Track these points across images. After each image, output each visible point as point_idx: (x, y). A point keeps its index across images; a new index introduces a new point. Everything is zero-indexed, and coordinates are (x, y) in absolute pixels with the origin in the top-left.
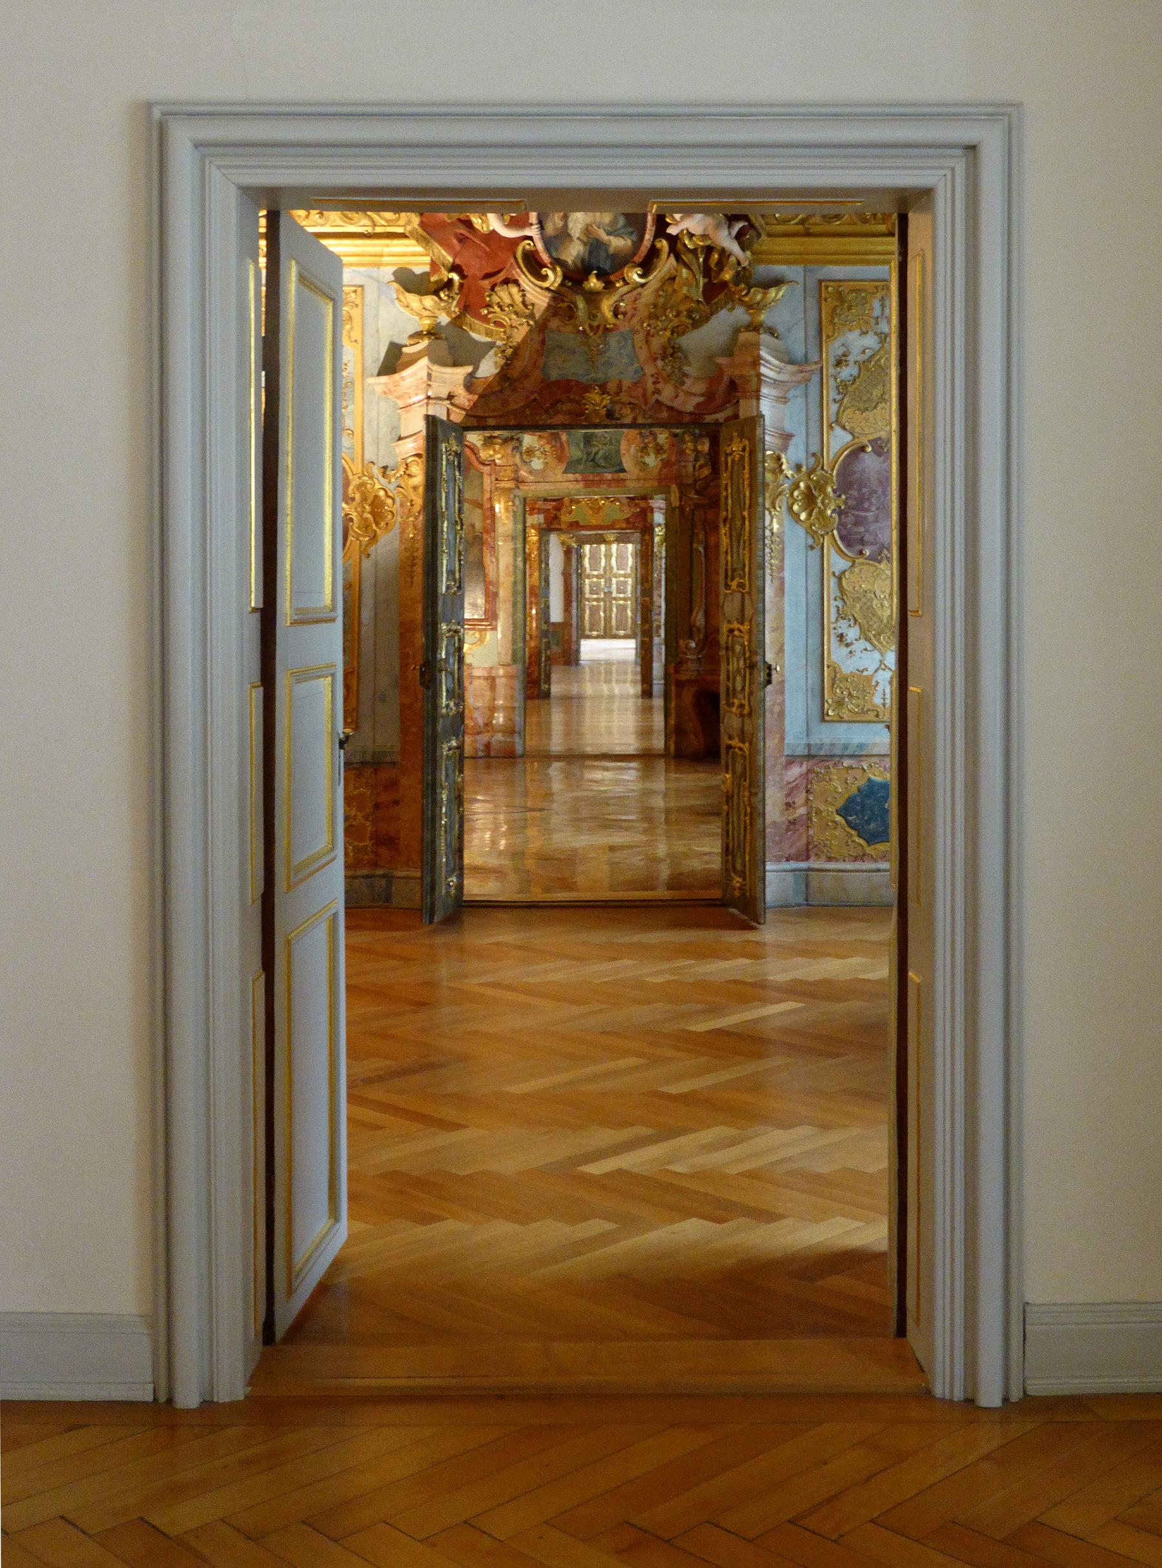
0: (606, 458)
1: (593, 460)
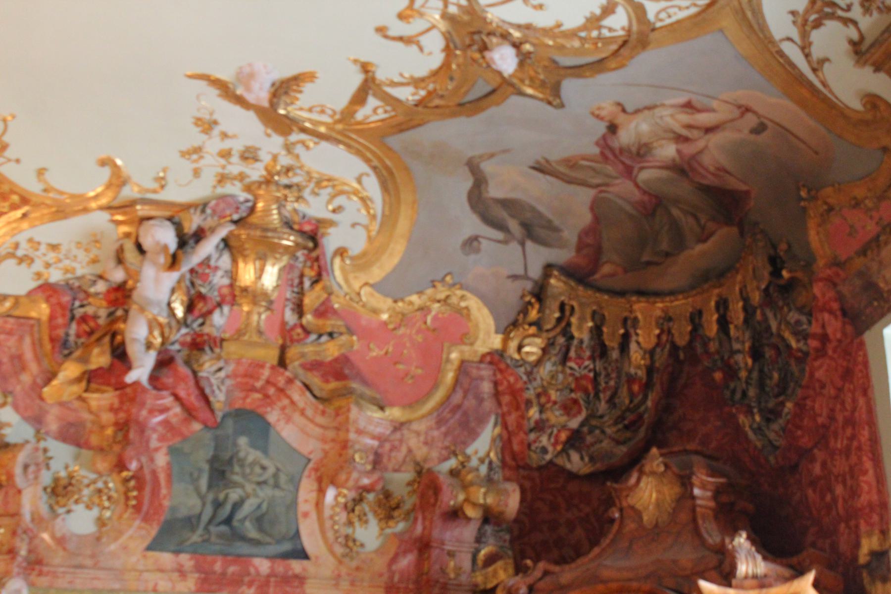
0: (259, 520)
1: (228, 521)
